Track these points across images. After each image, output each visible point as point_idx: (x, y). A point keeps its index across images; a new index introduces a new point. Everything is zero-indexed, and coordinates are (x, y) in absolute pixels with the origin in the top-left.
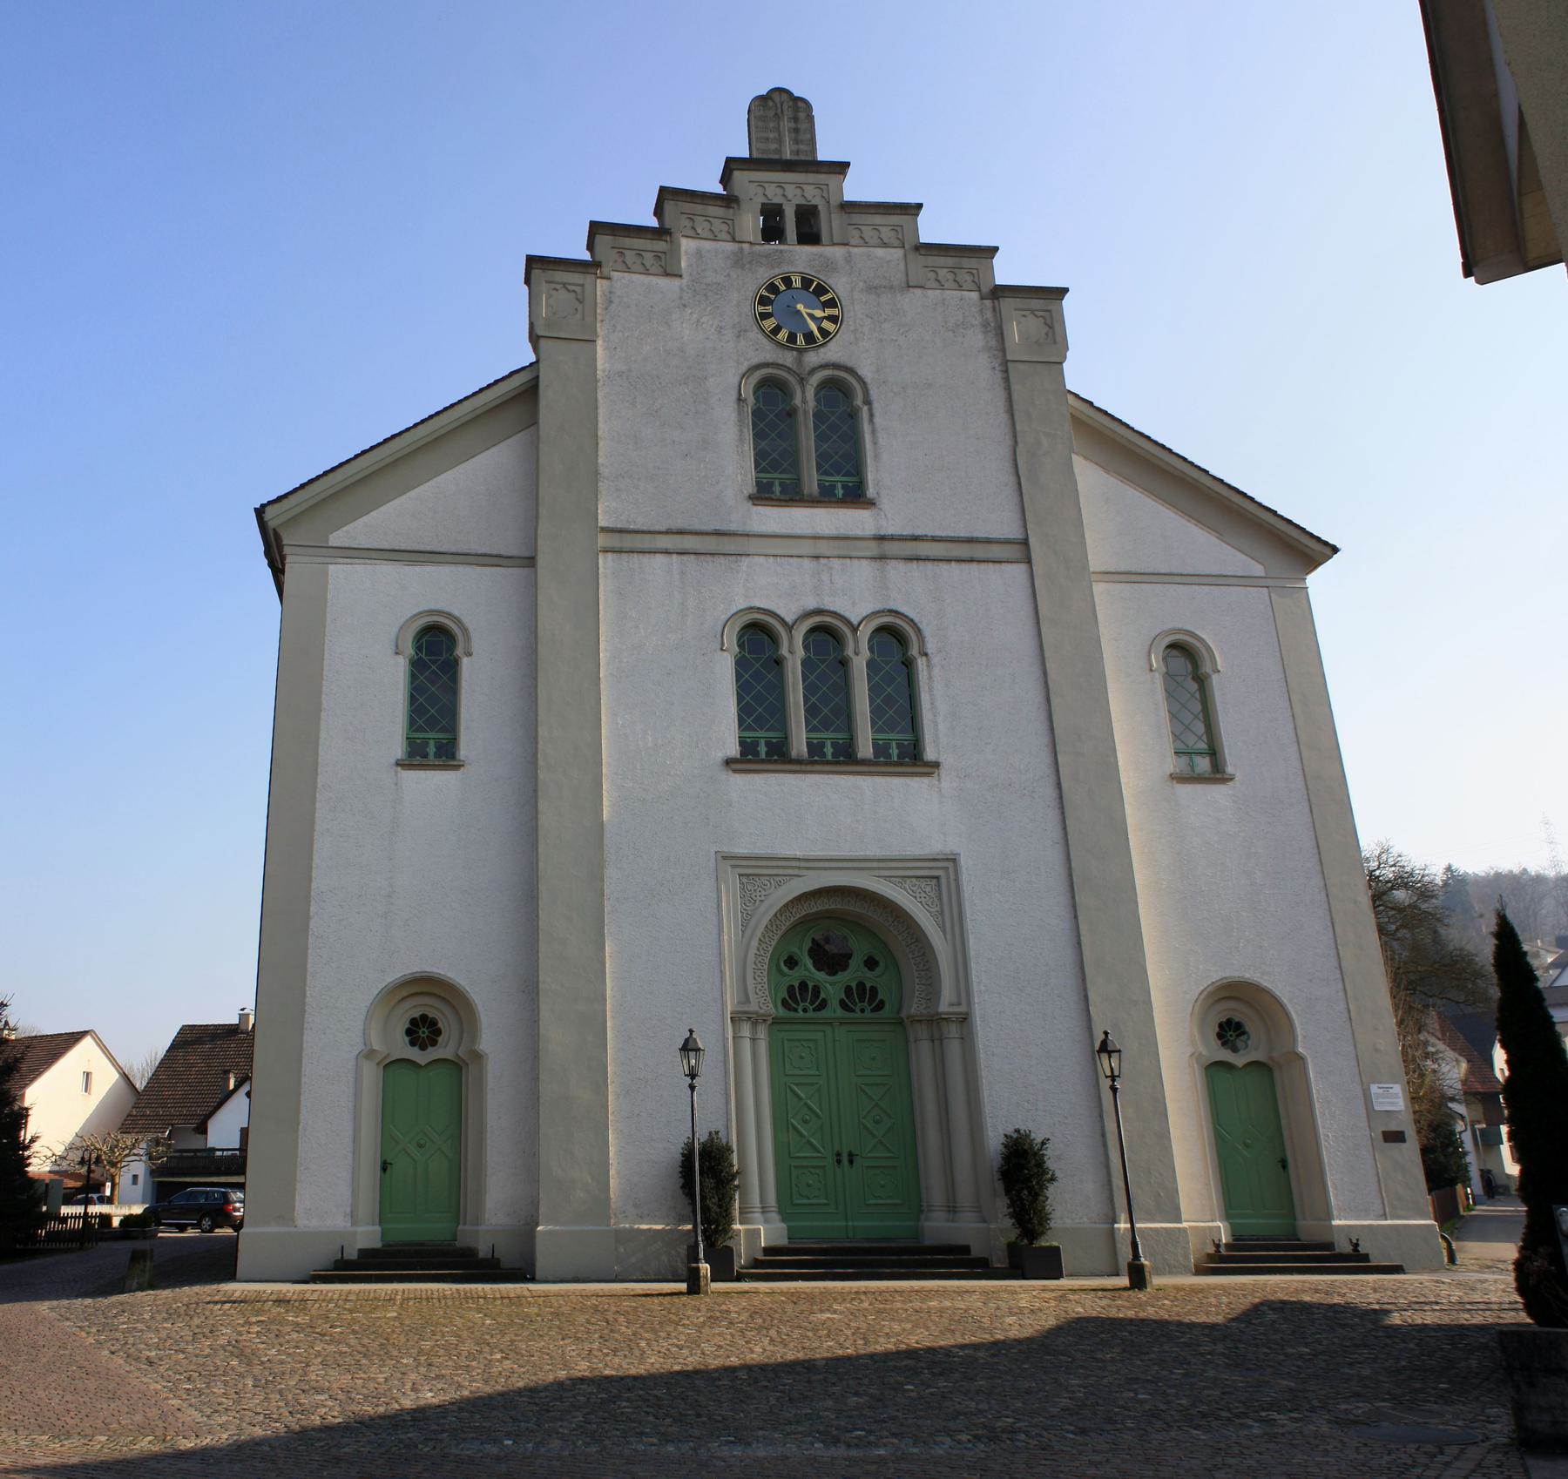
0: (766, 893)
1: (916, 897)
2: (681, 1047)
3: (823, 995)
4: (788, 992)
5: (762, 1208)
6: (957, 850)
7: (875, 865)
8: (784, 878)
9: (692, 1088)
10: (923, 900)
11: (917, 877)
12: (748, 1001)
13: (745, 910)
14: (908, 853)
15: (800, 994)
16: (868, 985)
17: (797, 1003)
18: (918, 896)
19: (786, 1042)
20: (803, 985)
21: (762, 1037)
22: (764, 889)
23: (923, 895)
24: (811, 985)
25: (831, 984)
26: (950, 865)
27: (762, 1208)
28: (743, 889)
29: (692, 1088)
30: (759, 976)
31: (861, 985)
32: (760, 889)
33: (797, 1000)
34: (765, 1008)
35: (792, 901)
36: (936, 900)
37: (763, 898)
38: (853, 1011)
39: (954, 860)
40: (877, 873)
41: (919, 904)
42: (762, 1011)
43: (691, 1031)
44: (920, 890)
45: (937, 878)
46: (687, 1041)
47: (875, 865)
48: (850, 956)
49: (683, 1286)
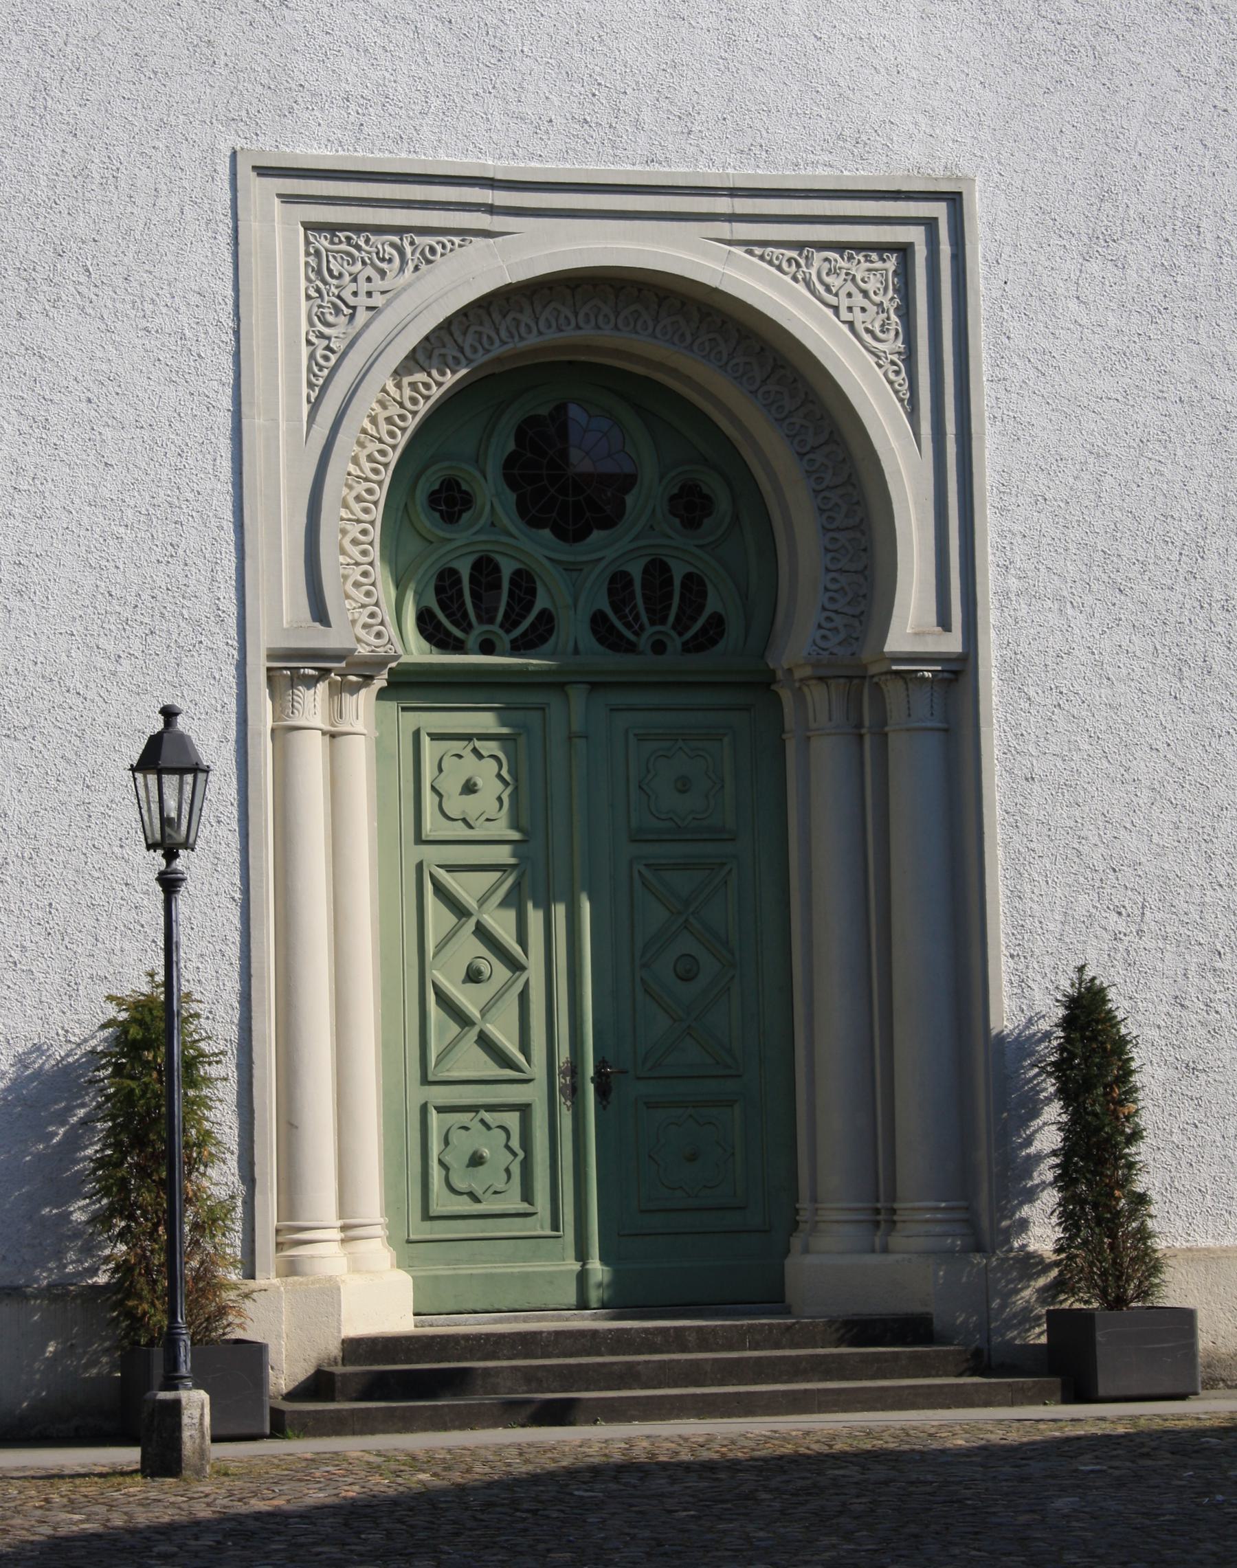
0: (385, 285)
1: (836, 309)
2: (135, 758)
3: (541, 602)
4: (439, 590)
5: (344, 1228)
6: (966, 168)
7: (722, 205)
8: (444, 239)
9: (170, 884)
10: (858, 317)
11: (840, 247)
12: (320, 613)
13: (321, 336)
14: (820, 171)
15: (474, 594)
16: (678, 572)
17: (468, 628)
18: (844, 303)
19: (426, 741)
20: (485, 568)
21: (359, 726)
22: (382, 273)
23: (859, 299)
24: (507, 568)
25: (570, 568)
26: (939, 210)
27: (344, 1228)
28: (319, 272)
29: (170, 884)
30: (355, 542)
31: (657, 570)
32: (369, 271)
33: (465, 615)
34: (371, 639)
35: (464, 312)
36: (894, 318)
37: (378, 300)
38: (631, 648)
39: (954, 200)
40: (724, 230)
41: (845, 328)
42: (362, 650)
43: (169, 714)
44: (850, 287)
45: (904, 251)
46: (155, 743)
47: (722, 205)
48: (628, 482)
49: (131, 1456)
